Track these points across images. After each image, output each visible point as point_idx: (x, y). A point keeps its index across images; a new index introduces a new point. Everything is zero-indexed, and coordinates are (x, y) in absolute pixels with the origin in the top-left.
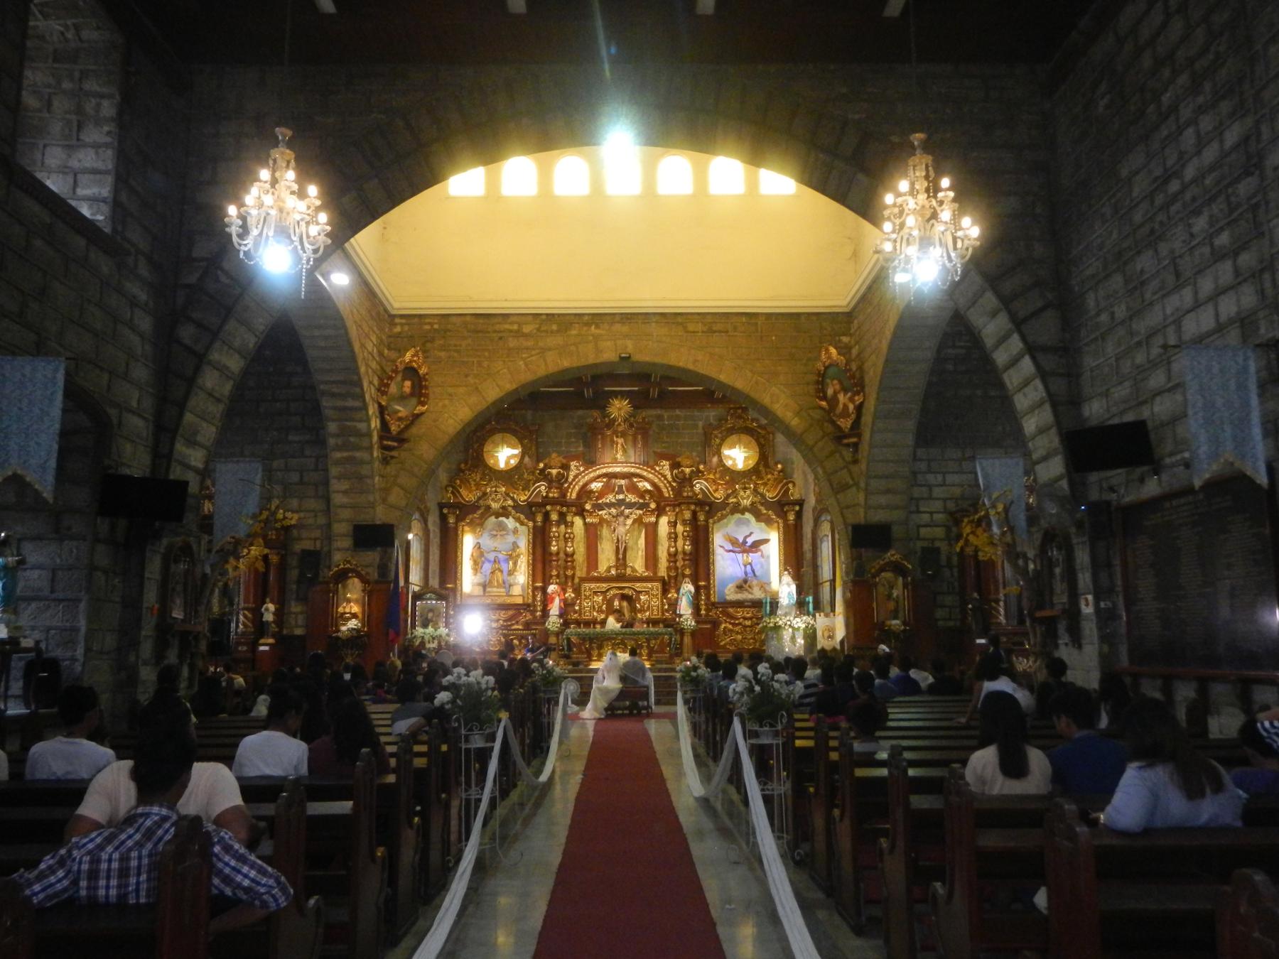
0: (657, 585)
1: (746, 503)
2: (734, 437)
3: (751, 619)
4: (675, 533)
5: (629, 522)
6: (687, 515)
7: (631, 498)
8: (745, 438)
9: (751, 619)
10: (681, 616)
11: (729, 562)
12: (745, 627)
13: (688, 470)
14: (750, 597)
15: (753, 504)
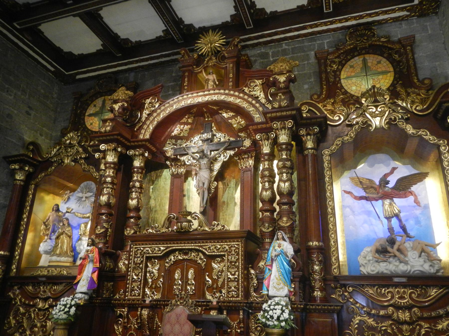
0: (237, 245)
1: (376, 122)
2: (357, 61)
3: (409, 308)
4: (271, 169)
5: (217, 166)
6: (283, 138)
7: (220, 137)
8: (372, 59)
9: (409, 308)
10: (270, 297)
11: (363, 217)
12: (398, 322)
13: (282, 79)
14: (402, 268)
15: (391, 122)
